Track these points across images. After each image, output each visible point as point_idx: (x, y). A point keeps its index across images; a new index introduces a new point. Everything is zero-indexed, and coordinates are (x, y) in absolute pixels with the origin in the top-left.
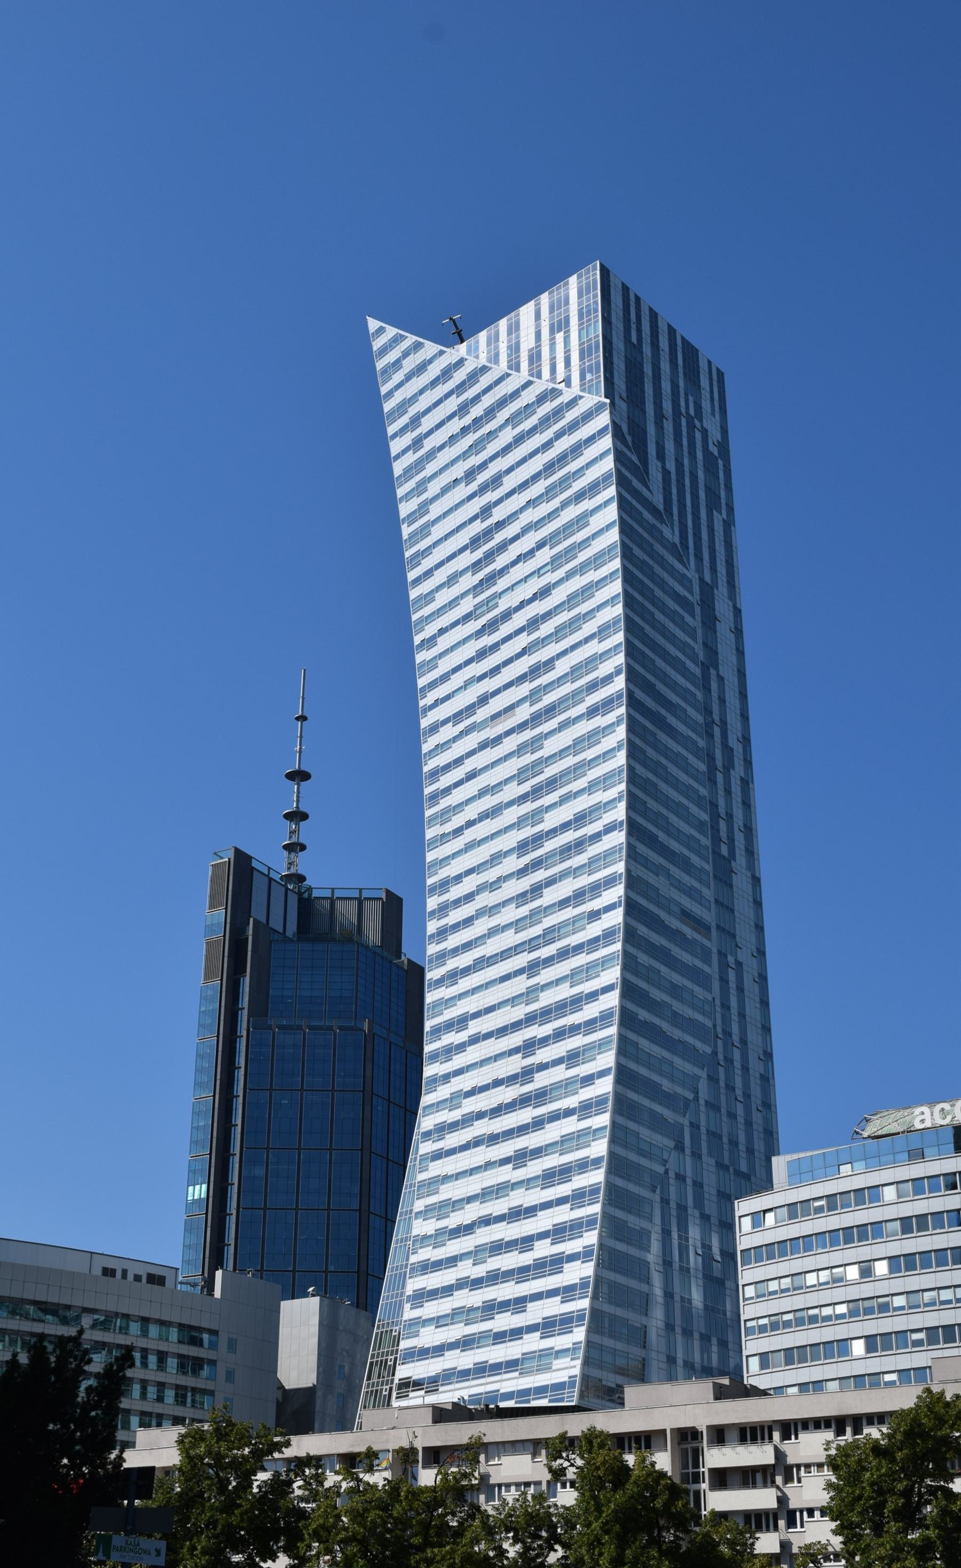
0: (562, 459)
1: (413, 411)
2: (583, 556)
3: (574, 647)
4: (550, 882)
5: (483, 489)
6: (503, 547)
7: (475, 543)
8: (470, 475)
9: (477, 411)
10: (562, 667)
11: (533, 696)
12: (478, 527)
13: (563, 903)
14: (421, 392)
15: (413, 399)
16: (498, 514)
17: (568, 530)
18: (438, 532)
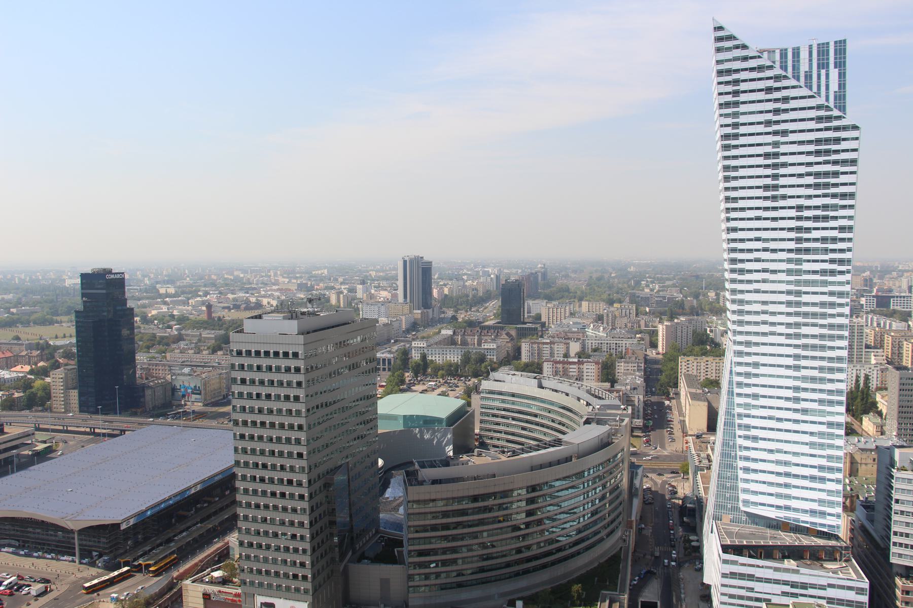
0: (827, 141)
1: (735, 76)
3: (824, 229)
4: (806, 325)
5: (776, 133)
6: (784, 165)
8: (768, 123)
10: (815, 234)
11: (799, 240)
12: (769, 149)
13: (814, 336)
14: (743, 70)
15: (737, 71)
16: (783, 149)
17: (826, 174)
18: (742, 140)
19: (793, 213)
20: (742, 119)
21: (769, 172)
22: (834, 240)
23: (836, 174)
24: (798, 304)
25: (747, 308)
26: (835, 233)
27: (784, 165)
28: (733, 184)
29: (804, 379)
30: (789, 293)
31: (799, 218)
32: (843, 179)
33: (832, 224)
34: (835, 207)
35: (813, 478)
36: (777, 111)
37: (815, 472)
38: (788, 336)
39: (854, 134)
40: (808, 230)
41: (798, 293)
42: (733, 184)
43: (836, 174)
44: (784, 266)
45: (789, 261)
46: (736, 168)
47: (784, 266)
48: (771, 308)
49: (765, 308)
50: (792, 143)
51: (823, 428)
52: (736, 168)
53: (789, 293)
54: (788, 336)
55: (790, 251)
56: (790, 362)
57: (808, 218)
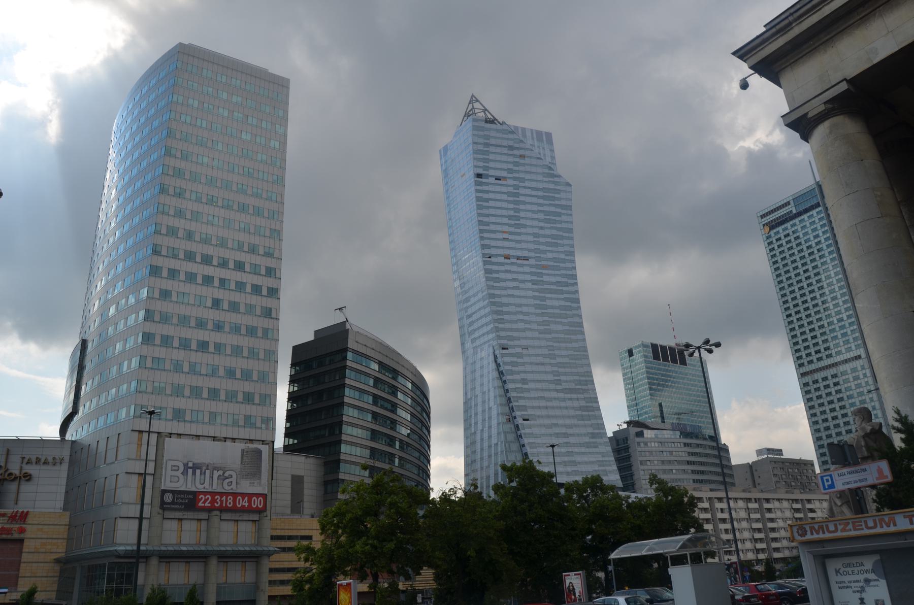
1: (486, 133)
2: (558, 225)
5: (515, 179)
6: (524, 203)
7: (509, 194)
9: (516, 152)
10: (549, 255)
12: (511, 189)
16: (522, 191)
19: (531, 238)
20: (491, 165)
21: (511, 206)
22: (564, 261)
23: (559, 214)
24: (547, 307)
25: (505, 309)
26: (562, 256)
27: (524, 203)
28: (485, 211)
29: (559, 365)
30: (534, 298)
31: (538, 243)
32: (564, 218)
33: (560, 249)
34: (562, 238)
35: (587, 445)
36: (516, 164)
37: (587, 439)
38: (541, 332)
39: (568, 189)
40: (545, 252)
41: (544, 299)
42: (485, 211)
43: (559, 214)
44: (528, 277)
45: (532, 273)
46: (487, 200)
47: (528, 277)
48: (525, 309)
49: (519, 309)
50: (529, 188)
51: (583, 403)
52: (487, 200)
53: (534, 298)
54: (541, 332)
55: (531, 266)
56: (546, 352)
57: (543, 244)
